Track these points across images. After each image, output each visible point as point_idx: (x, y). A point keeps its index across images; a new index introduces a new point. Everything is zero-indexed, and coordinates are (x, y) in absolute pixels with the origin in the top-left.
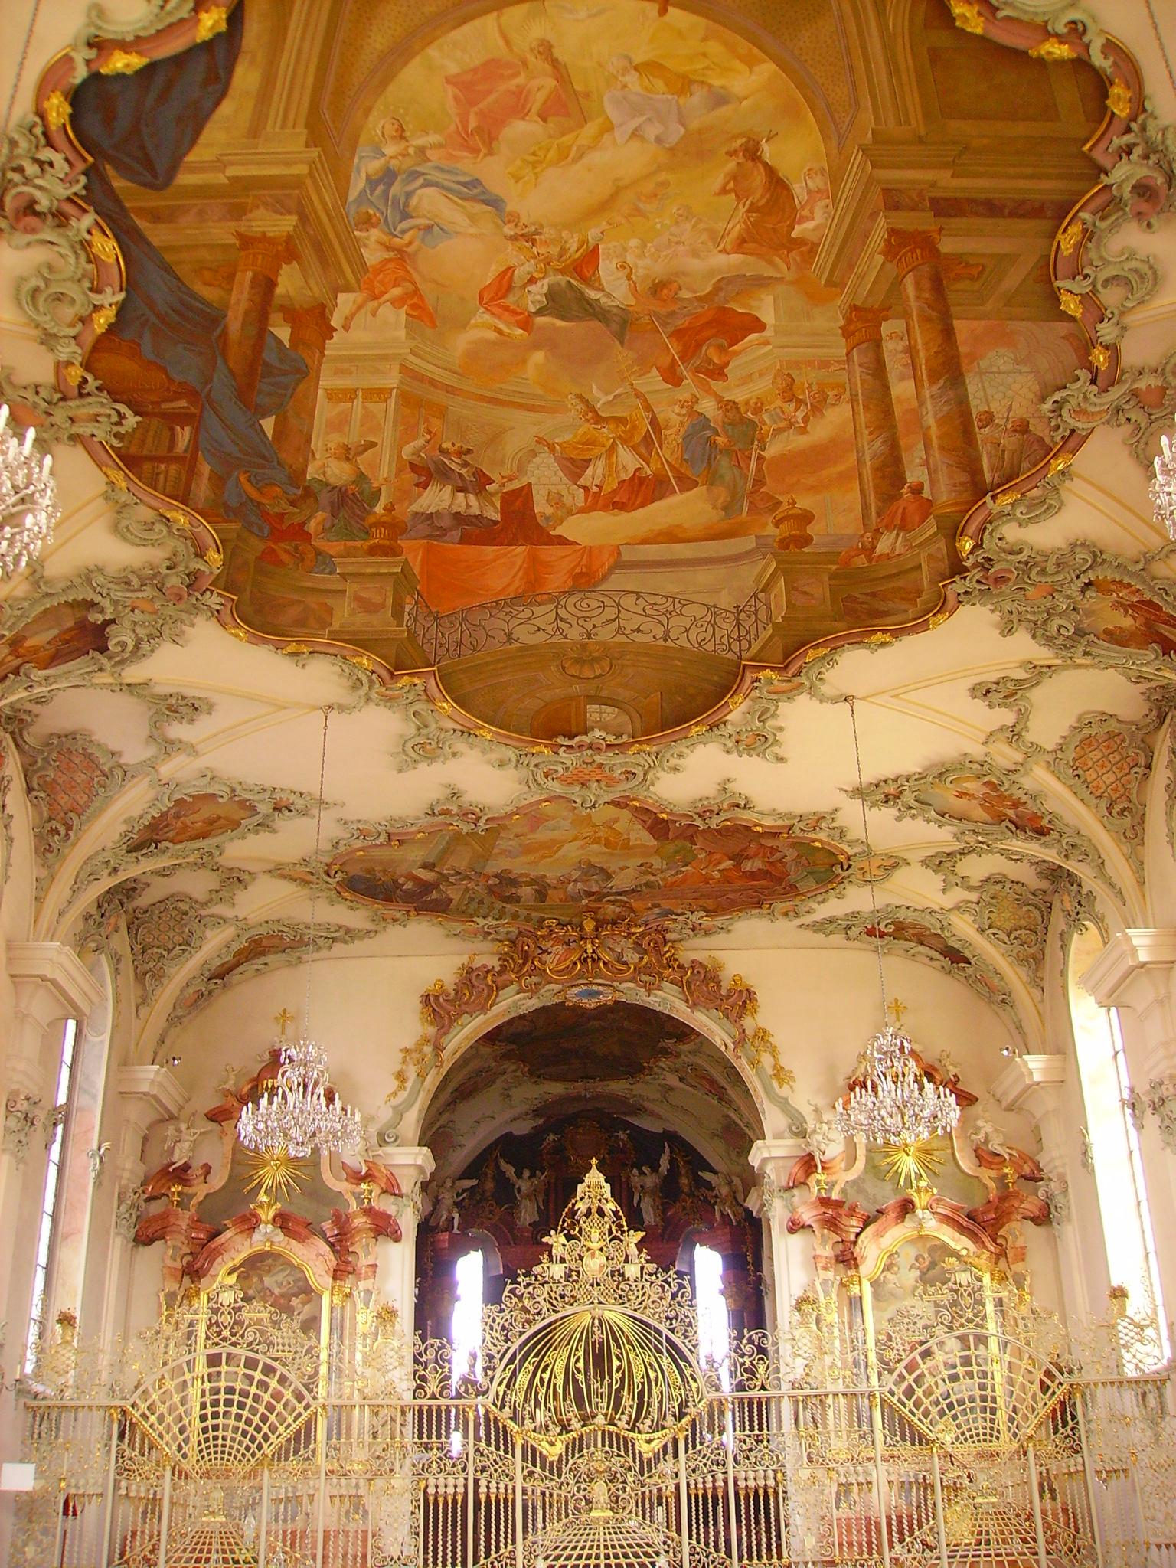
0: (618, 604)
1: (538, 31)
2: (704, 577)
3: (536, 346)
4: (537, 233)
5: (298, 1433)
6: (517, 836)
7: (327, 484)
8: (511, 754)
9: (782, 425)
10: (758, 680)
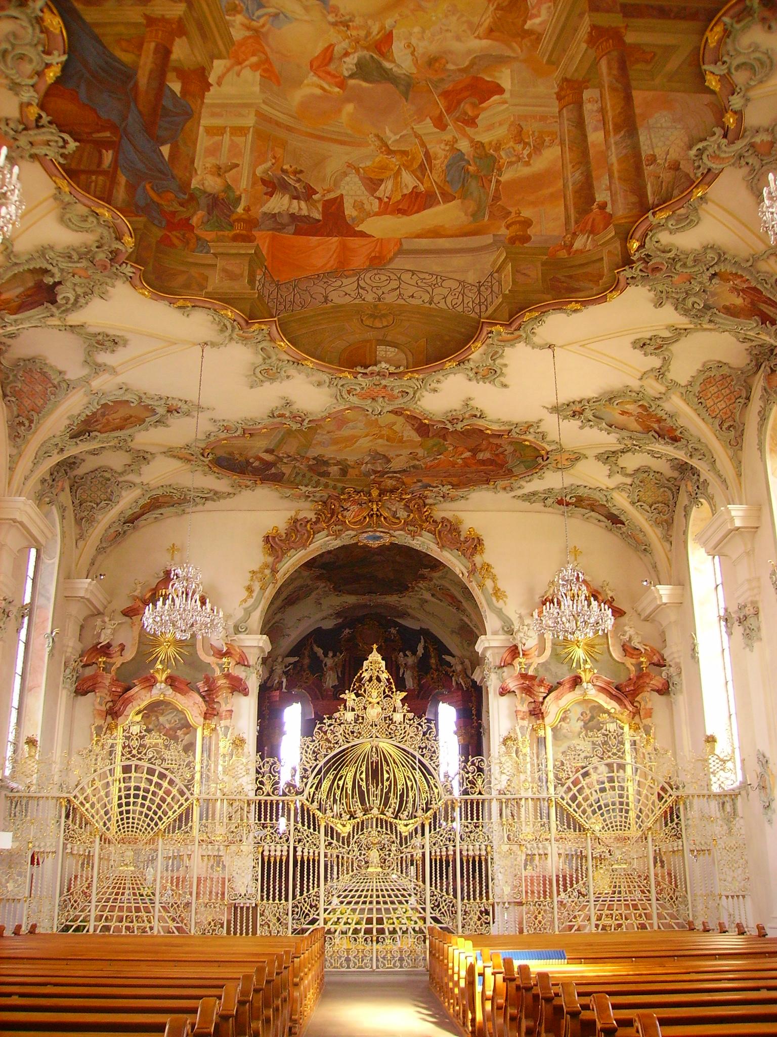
0: (399, 278)
2: (458, 261)
3: (348, 100)
4: (351, 21)
5: (181, 815)
6: (328, 432)
7: (205, 192)
8: (325, 377)
9: (514, 159)
10: (491, 332)
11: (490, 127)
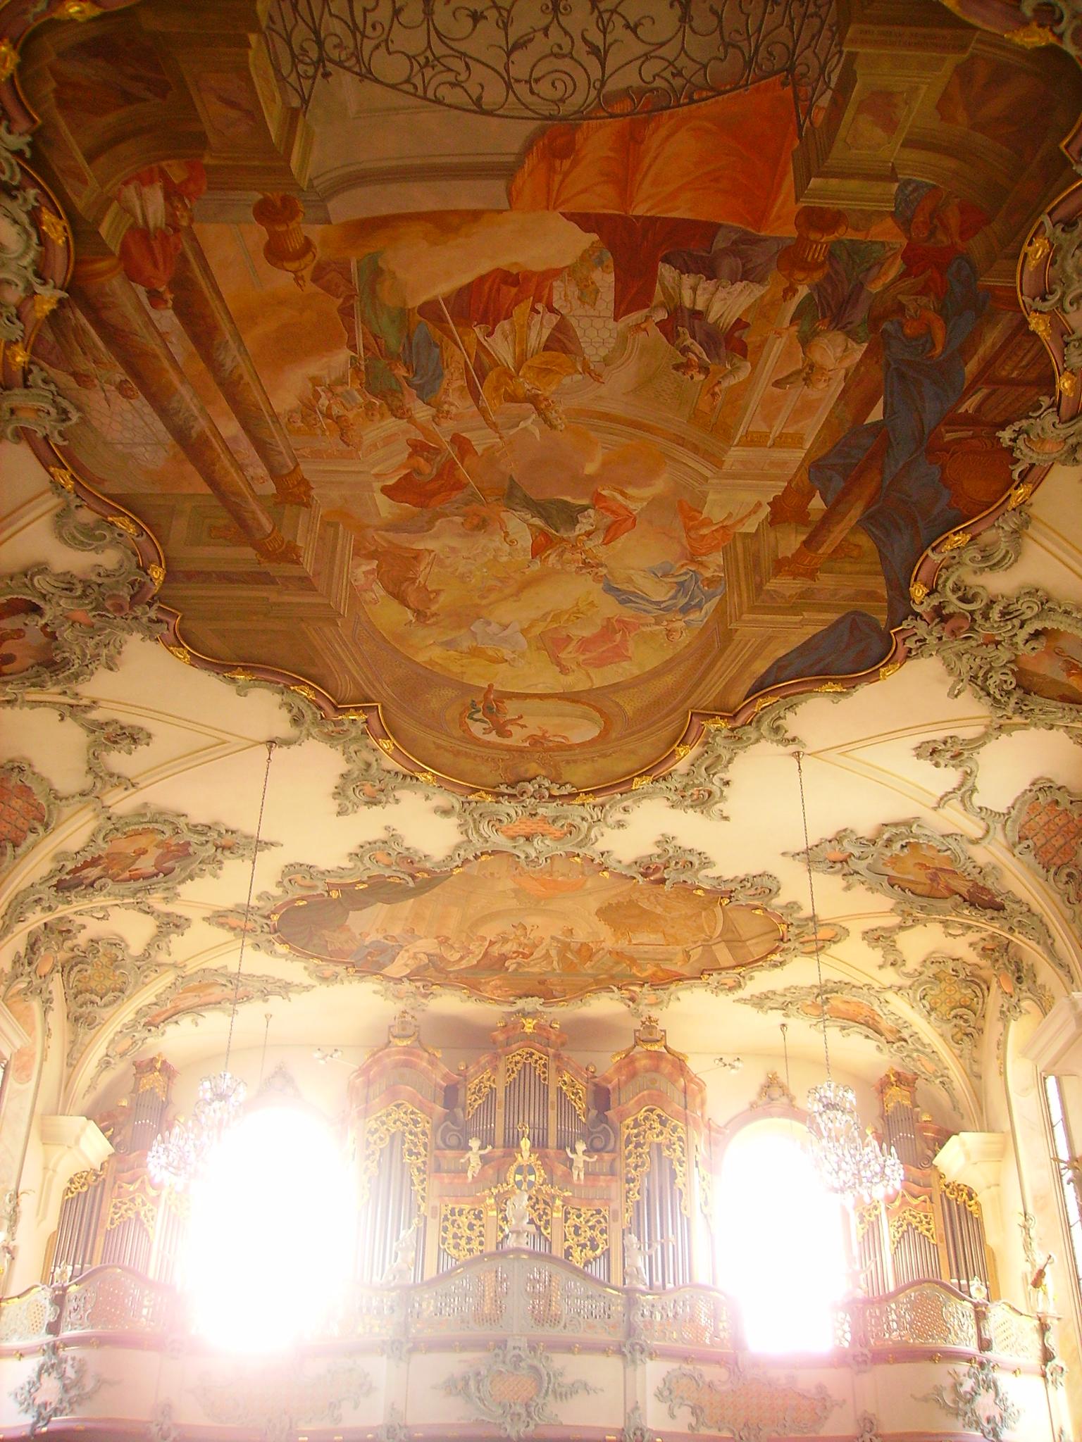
0: (509, 86)
1: (570, 679)
3: (591, 478)
4: (581, 568)
9: (339, 389)
11: (388, 440)
